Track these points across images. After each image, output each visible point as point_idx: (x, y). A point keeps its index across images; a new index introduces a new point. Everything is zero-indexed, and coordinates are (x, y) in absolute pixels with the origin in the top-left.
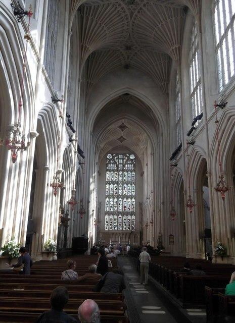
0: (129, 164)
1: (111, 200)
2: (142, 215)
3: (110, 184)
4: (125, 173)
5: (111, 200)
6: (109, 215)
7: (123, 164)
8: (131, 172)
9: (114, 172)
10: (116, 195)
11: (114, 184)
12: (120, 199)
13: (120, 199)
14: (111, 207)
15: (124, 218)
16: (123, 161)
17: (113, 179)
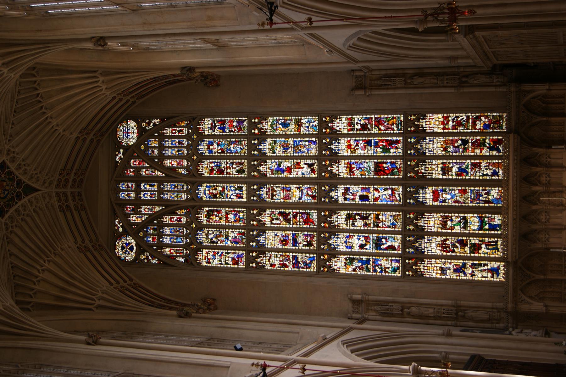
0: (162, 147)
1: (340, 242)
2: (420, 73)
3: (262, 250)
4: (205, 168)
5: (340, 242)
6: (421, 256)
7: (160, 181)
8: (202, 137)
9: (201, 227)
10: (315, 217)
11: (262, 229)
12: (338, 194)
13: (338, 194)
14: (378, 244)
15: (437, 174)
16: (149, 180)
17: (234, 234)
